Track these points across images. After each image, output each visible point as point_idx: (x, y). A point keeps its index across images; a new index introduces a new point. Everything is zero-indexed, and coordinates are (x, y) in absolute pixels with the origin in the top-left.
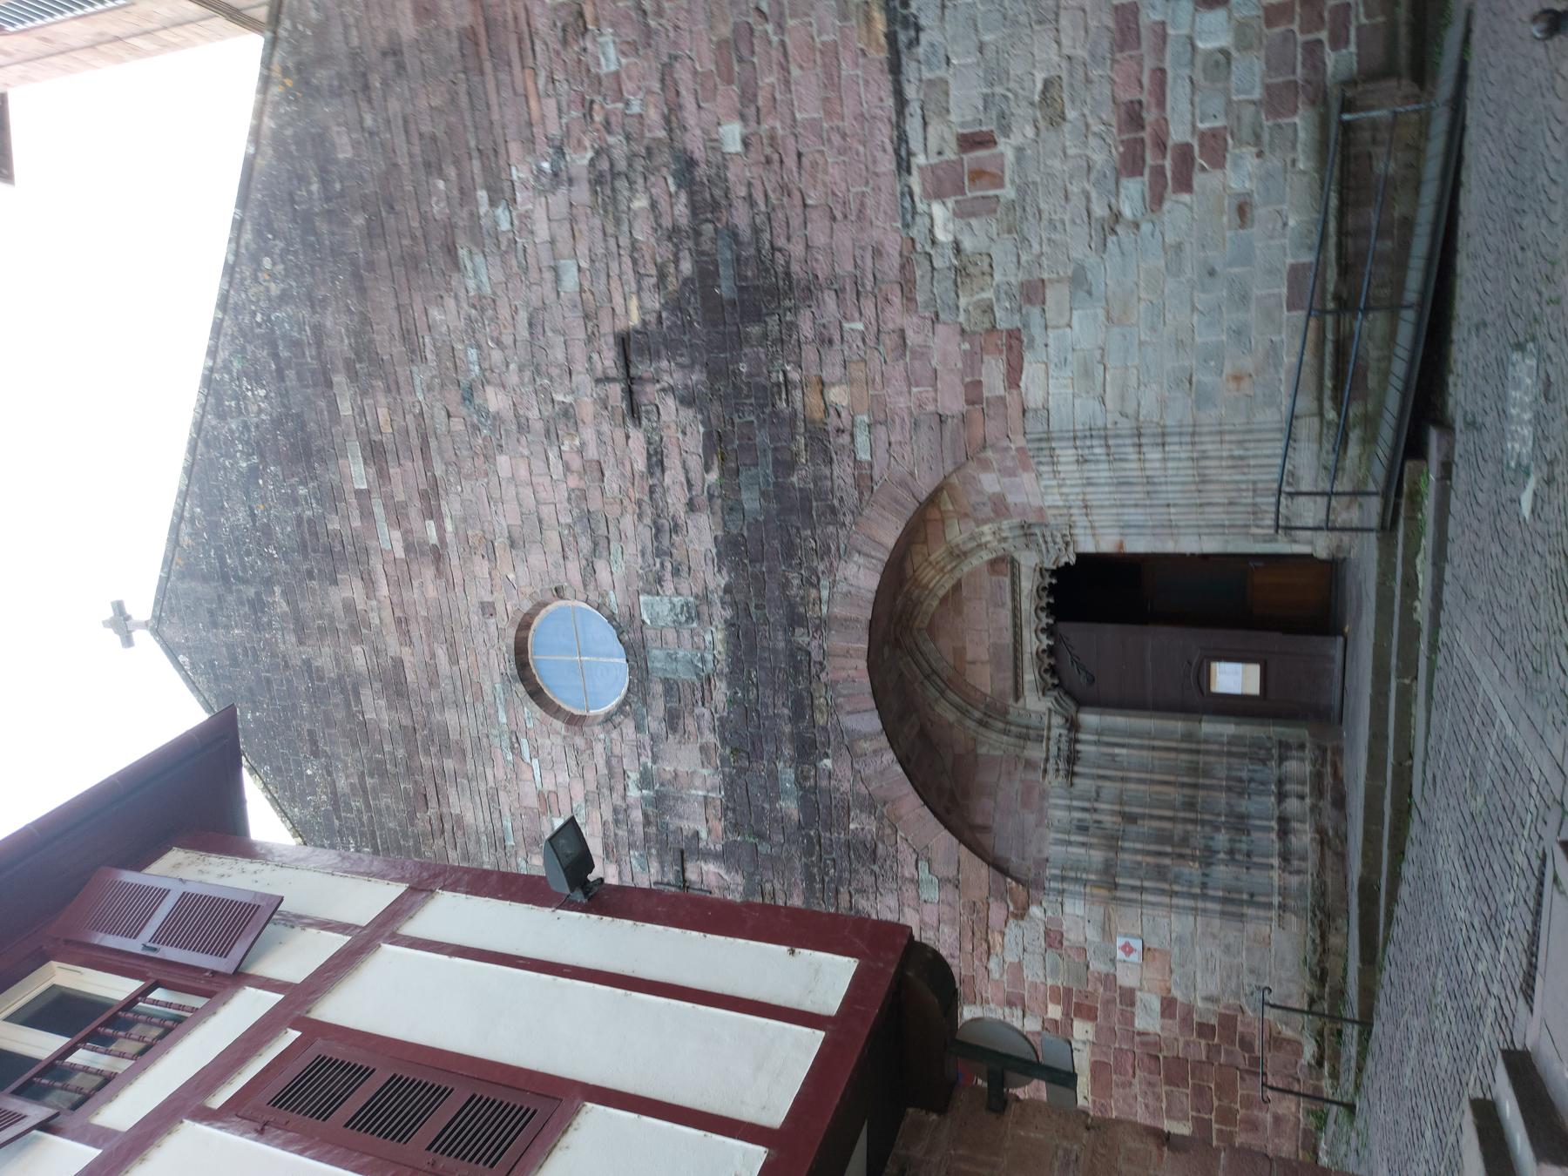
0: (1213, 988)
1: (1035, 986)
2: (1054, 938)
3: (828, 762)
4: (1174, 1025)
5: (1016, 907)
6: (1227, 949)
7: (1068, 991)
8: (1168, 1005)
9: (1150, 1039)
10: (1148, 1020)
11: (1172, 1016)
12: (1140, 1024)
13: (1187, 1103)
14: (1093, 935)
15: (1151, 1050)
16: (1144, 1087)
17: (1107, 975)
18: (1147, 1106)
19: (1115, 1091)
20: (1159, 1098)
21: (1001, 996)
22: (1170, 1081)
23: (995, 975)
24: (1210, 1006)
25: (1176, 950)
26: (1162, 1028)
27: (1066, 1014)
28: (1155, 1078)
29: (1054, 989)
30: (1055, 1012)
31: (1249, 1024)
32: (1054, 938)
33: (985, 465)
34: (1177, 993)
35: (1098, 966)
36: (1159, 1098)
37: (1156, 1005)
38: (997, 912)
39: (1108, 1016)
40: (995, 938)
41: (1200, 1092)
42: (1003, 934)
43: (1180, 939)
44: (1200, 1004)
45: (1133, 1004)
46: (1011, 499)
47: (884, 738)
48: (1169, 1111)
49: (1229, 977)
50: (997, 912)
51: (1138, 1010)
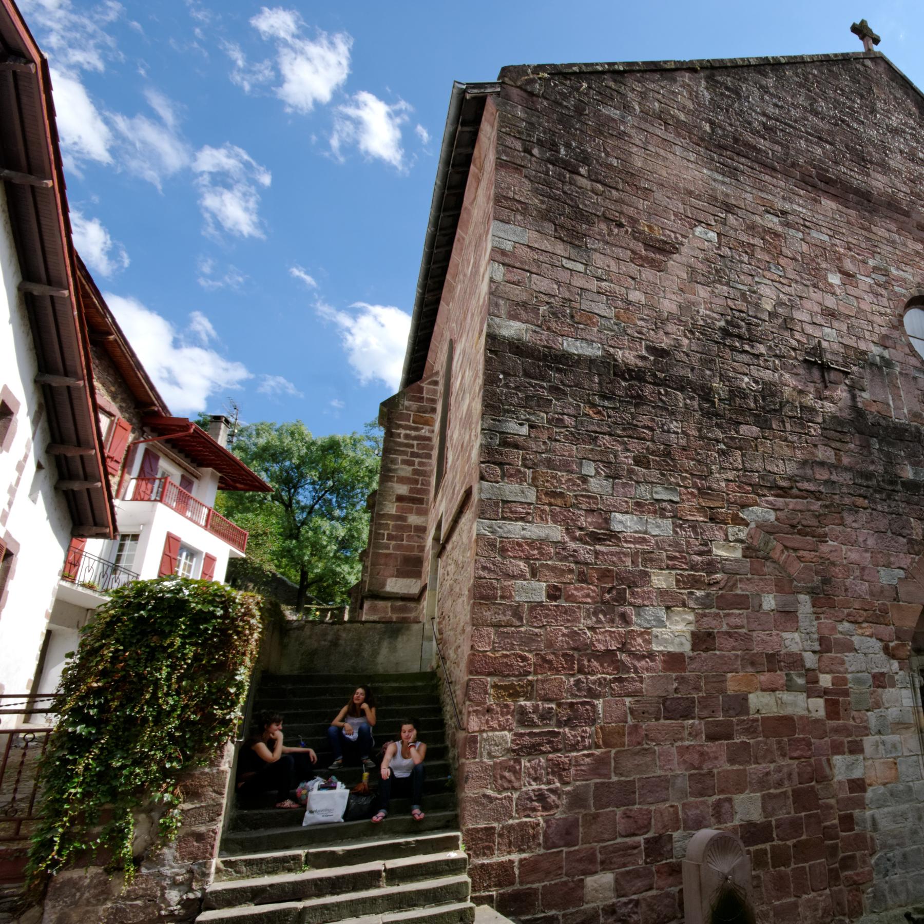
0: (885, 824)
1: (843, 663)
2: (881, 681)
4: (845, 794)
5: (893, 648)
7: (846, 693)
8: (858, 785)
10: (842, 768)
11: (852, 790)
13: (782, 815)
14: (893, 713)
15: (821, 776)
17: (866, 728)
18: (768, 774)
19: (773, 741)
20: (780, 784)
21: (826, 633)
22: (796, 793)
23: (840, 627)
24: (869, 824)
26: (839, 782)
27: (826, 692)
28: (795, 777)
29: (844, 681)
30: (826, 680)
32: (881, 681)
36: (780, 784)
37: (857, 774)
38: (887, 631)
40: (868, 629)
41: (795, 826)
42: (871, 636)
43: (910, 789)
44: (868, 813)
48: (771, 797)
50: (887, 631)
51: (849, 758)
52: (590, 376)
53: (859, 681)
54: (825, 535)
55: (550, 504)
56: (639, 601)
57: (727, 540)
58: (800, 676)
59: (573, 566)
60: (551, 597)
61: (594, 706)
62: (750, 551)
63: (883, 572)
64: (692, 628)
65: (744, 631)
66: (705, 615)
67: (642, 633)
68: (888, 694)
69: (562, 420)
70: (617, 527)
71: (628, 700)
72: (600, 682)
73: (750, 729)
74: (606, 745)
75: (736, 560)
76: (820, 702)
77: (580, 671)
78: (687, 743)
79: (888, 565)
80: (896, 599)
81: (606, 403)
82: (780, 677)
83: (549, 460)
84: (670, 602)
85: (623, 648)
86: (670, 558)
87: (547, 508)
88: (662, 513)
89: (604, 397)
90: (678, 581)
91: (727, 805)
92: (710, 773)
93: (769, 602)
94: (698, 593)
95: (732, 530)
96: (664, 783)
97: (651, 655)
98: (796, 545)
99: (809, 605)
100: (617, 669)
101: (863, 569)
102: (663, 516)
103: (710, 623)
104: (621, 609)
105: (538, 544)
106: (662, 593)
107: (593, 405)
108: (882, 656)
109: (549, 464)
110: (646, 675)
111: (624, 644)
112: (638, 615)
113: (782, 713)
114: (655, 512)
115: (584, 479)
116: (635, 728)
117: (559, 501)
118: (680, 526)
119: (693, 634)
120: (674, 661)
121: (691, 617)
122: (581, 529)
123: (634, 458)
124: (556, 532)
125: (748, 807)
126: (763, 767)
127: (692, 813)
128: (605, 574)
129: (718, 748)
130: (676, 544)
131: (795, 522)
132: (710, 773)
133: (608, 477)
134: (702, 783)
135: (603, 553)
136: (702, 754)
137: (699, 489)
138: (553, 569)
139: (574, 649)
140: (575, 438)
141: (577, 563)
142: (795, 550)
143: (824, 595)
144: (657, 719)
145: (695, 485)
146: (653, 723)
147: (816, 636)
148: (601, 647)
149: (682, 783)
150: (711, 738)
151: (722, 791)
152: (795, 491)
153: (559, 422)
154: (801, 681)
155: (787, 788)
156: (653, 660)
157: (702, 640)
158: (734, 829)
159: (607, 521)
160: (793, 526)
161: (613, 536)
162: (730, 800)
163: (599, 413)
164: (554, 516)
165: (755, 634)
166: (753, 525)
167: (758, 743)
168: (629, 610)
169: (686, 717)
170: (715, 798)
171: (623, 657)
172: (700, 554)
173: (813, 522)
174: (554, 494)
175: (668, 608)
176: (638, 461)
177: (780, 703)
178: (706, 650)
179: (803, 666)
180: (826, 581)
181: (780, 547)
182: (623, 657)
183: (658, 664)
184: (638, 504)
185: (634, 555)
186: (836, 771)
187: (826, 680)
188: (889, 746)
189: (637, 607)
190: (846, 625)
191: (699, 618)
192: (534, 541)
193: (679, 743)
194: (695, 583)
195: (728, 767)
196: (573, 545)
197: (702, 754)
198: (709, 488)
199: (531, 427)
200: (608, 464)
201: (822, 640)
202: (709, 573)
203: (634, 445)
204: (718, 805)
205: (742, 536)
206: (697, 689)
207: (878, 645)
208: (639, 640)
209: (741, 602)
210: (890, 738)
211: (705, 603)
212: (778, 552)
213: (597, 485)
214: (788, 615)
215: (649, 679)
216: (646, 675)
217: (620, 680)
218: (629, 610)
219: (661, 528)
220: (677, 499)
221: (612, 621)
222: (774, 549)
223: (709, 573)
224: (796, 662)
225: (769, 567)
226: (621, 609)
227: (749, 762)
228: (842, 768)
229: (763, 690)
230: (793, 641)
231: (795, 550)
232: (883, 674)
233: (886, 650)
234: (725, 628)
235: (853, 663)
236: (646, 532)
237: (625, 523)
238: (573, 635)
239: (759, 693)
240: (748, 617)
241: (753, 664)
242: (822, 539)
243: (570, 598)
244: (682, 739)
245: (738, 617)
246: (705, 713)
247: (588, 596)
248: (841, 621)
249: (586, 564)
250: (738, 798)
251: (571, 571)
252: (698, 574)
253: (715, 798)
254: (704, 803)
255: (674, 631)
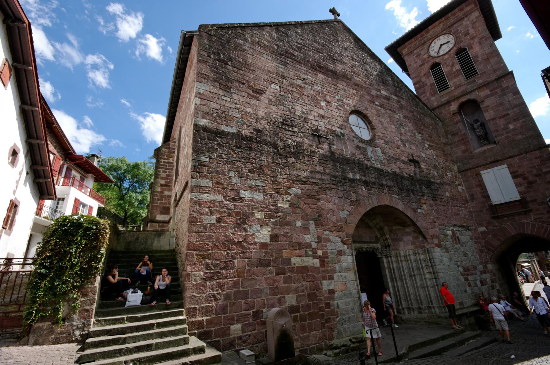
1: (326, 246)
2: (340, 253)
3: (364, 189)
6: (353, 309)
7: (327, 257)
9: (321, 286)
10: (326, 285)
12: (324, 282)
14: (345, 265)
15: (318, 288)
16: (305, 286)
17: (335, 270)
18: (298, 287)
19: (300, 275)
20: (303, 291)
21: (320, 235)
22: (309, 295)
23: (325, 233)
25: (348, 292)
27: (320, 257)
28: (308, 288)
29: (327, 253)
30: (320, 253)
31: (334, 320)
32: (340, 253)
33: (415, 238)
34: (336, 295)
35: (337, 266)
36: (303, 291)
37: (331, 287)
39: (324, 271)
40: (336, 233)
45: (329, 279)
46: (401, 243)
47: (373, 206)
48: (299, 296)
49: (345, 311)
51: (329, 282)
52: (232, 139)
53: (332, 253)
54: (320, 199)
55: (217, 187)
56: (250, 223)
57: (283, 200)
58: (310, 251)
59: (226, 210)
60: (218, 222)
61: (234, 262)
62: (291, 205)
63: (341, 212)
64: (270, 233)
65: (289, 234)
66: (275, 228)
67: (251, 235)
68: (343, 258)
69: (222, 156)
70: (242, 196)
71: (246, 260)
72: (236, 253)
73: (292, 271)
74: (238, 276)
75: (287, 208)
76: (318, 261)
77: (229, 249)
78: (268, 276)
79: (343, 210)
80: (346, 222)
81: (238, 150)
82: (303, 251)
83: (217, 171)
84: (262, 224)
85: (245, 241)
86: (262, 207)
87: (216, 189)
88: (259, 190)
89: (237, 147)
90: (265, 216)
91: (283, 299)
92: (277, 287)
93: (299, 224)
94: (272, 220)
95: (285, 197)
96: (260, 291)
97: (255, 243)
98: (309, 202)
99: (314, 224)
100: (242, 248)
101: (334, 211)
102: (259, 192)
103: (277, 232)
104: (244, 226)
105: (213, 202)
106: (259, 220)
107: (233, 150)
108: (341, 244)
109: (217, 172)
110: (253, 251)
111: (245, 239)
112: (250, 228)
113: (304, 265)
114: (256, 190)
115: (230, 178)
116: (249, 270)
117: (221, 186)
118: (266, 195)
119: (270, 235)
120: (263, 245)
121: (270, 229)
122: (229, 196)
123: (249, 170)
124: (220, 198)
125: (291, 300)
126: (296, 285)
127: (270, 302)
128: (238, 213)
129: (280, 278)
130: (264, 202)
131: (308, 194)
132: (277, 287)
133: (239, 177)
134: (274, 291)
135: (237, 205)
136: (274, 280)
137: (273, 182)
138: (218, 211)
139: (226, 241)
140: (227, 163)
141: (227, 209)
142: (308, 204)
143: (319, 221)
144: (257, 267)
145: (271, 180)
146: (256, 268)
147: (316, 236)
148: (236, 240)
149: (267, 291)
150: (277, 274)
151: (281, 294)
152: (308, 182)
153: (221, 157)
154: (311, 253)
155: (305, 293)
156: (256, 245)
157: (274, 238)
158: (286, 308)
159: (239, 193)
160: (308, 195)
161: (241, 199)
162: (284, 297)
163: (235, 153)
164: (219, 191)
165: (293, 235)
166: (293, 195)
167: (295, 276)
168: (247, 226)
169: (268, 266)
170: (279, 296)
171: (245, 244)
172: (273, 206)
173: (316, 194)
174: (218, 184)
175: (261, 226)
176: (250, 171)
177: (303, 261)
178: (276, 241)
179: (311, 247)
180: (320, 216)
181: (303, 203)
182: (245, 244)
183: (258, 247)
184: (250, 187)
185: (249, 206)
186: (324, 286)
187: (320, 253)
188: (343, 277)
189: (250, 225)
190: (327, 232)
191: (273, 229)
192: (211, 201)
193: (265, 276)
194: (271, 216)
195: (283, 285)
196: (226, 202)
197: (274, 280)
198: (277, 181)
199: (210, 158)
200: (239, 172)
201: (318, 238)
202: (277, 213)
203: (248, 165)
204: (280, 299)
205: (289, 199)
206: (272, 256)
207: (339, 239)
208: (251, 238)
209: (288, 224)
210: (344, 274)
211: (275, 224)
212: (302, 205)
213: (235, 180)
214: (306, 229)
215: (254, 252)
216: (253, 251)
217: (243, 253)
218: (247, 226)
219: (258, 196)
220: (264, 185)
221: (240, 231)
222: (300, 204)
223: (277, 213)
224: (309, 246)
225: (299, 211)
226: (244, 226)
227: (291, 283)
228: (326, 285)
229: (297, 256)
230: (308, 238)
231: (308, 204)
232: (341, 250)
233: (342, 241)
234: (282, 233)
235: (330, 246)
236: (253, 198)
237: (245, 194)
238: (226, 236)
239: (295, 257)
240: (291, 229)
241: (293, 246)
242: (319, 200)
243: (225, 222)
244: (266, 275)
245: (287, 229)
246: (275, 265)
247: (231, 221)
248: (325, 231)
249: (231, 209)
250: (287, 296)
251: (225, 212)
252: (272, 213)
253: (279, 296)
254: (275, 298)
255: (263, 234)
